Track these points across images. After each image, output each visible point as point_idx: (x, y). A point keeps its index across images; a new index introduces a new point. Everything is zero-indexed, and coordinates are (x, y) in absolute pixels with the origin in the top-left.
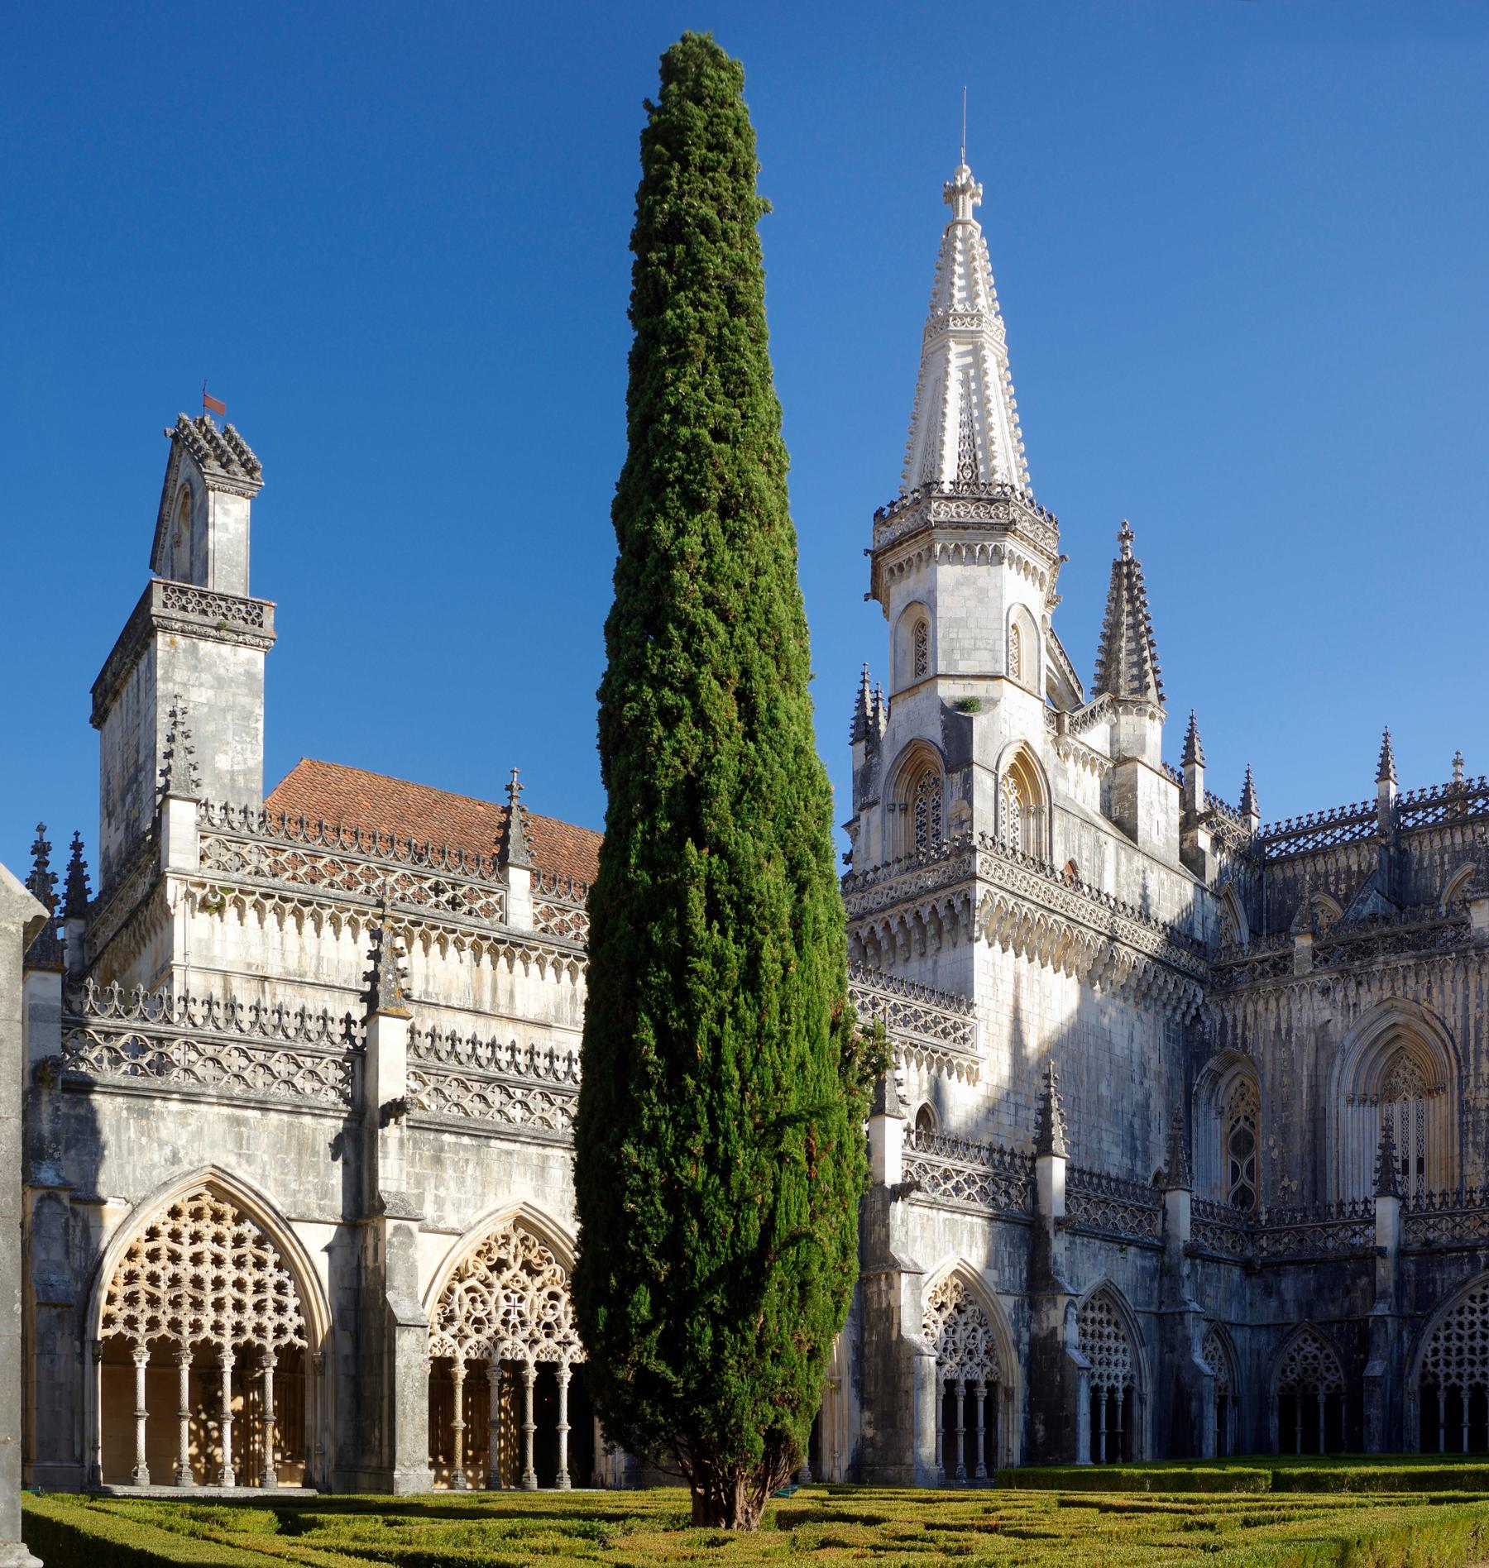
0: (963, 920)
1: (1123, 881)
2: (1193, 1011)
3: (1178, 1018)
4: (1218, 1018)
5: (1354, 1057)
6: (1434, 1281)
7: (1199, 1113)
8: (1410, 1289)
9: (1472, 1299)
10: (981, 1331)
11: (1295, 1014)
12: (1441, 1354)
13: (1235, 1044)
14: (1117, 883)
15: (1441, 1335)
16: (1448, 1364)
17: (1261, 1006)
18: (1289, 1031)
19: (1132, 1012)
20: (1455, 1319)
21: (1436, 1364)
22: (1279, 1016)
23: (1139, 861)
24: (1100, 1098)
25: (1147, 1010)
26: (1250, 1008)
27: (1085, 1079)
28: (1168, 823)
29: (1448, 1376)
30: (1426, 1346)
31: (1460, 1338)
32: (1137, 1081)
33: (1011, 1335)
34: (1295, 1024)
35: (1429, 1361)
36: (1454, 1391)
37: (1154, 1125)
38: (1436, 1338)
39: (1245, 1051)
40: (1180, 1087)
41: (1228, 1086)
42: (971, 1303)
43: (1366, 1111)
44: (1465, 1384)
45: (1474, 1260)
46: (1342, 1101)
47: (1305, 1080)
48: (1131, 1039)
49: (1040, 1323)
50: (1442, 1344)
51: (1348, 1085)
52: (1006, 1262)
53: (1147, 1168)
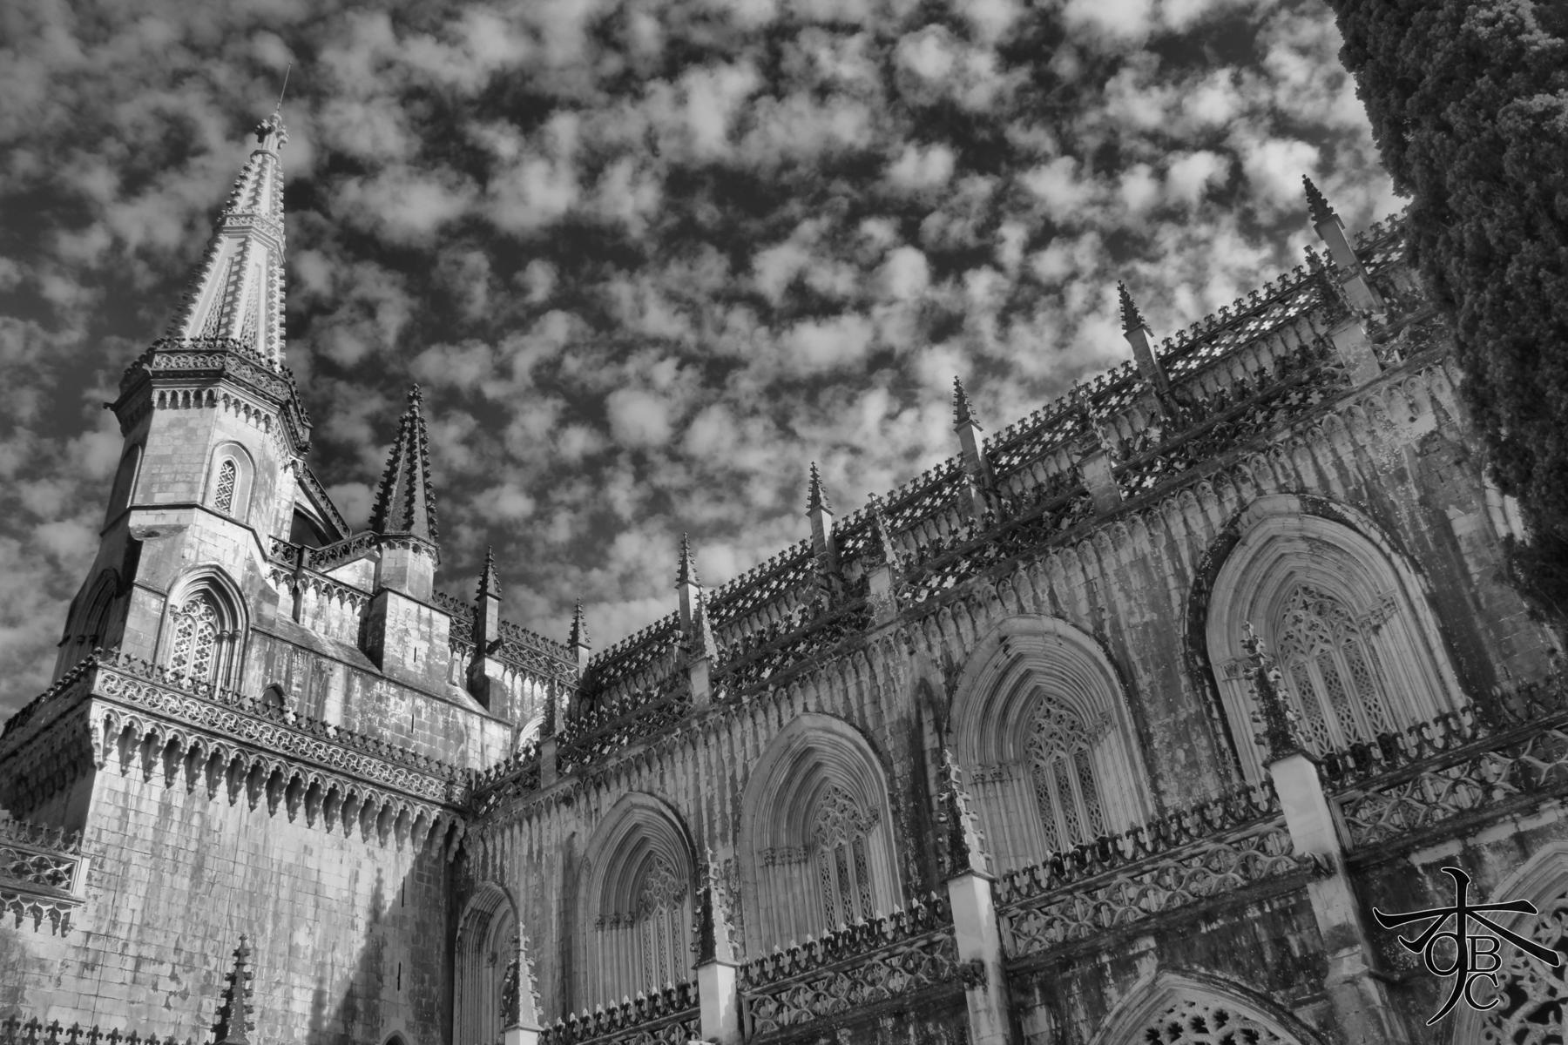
1: (354, 708)
2: (455, 846)
3: (435, 854)
4: (481, 849)
5: (601, 871)
7: (465, 962)
11: (545, 833)
13: (494, 877)
14: (346, 710)
22: (531, 839)
24: (293, 950)
27: (269, 927)
34: (545, 844)
37: (389, 981)
39: (502, 885)
40: (438, 935)
41: (499, 927)
43: (623, 934)
46: (590, 928)
47: (554, 906)
51: (596, 906)
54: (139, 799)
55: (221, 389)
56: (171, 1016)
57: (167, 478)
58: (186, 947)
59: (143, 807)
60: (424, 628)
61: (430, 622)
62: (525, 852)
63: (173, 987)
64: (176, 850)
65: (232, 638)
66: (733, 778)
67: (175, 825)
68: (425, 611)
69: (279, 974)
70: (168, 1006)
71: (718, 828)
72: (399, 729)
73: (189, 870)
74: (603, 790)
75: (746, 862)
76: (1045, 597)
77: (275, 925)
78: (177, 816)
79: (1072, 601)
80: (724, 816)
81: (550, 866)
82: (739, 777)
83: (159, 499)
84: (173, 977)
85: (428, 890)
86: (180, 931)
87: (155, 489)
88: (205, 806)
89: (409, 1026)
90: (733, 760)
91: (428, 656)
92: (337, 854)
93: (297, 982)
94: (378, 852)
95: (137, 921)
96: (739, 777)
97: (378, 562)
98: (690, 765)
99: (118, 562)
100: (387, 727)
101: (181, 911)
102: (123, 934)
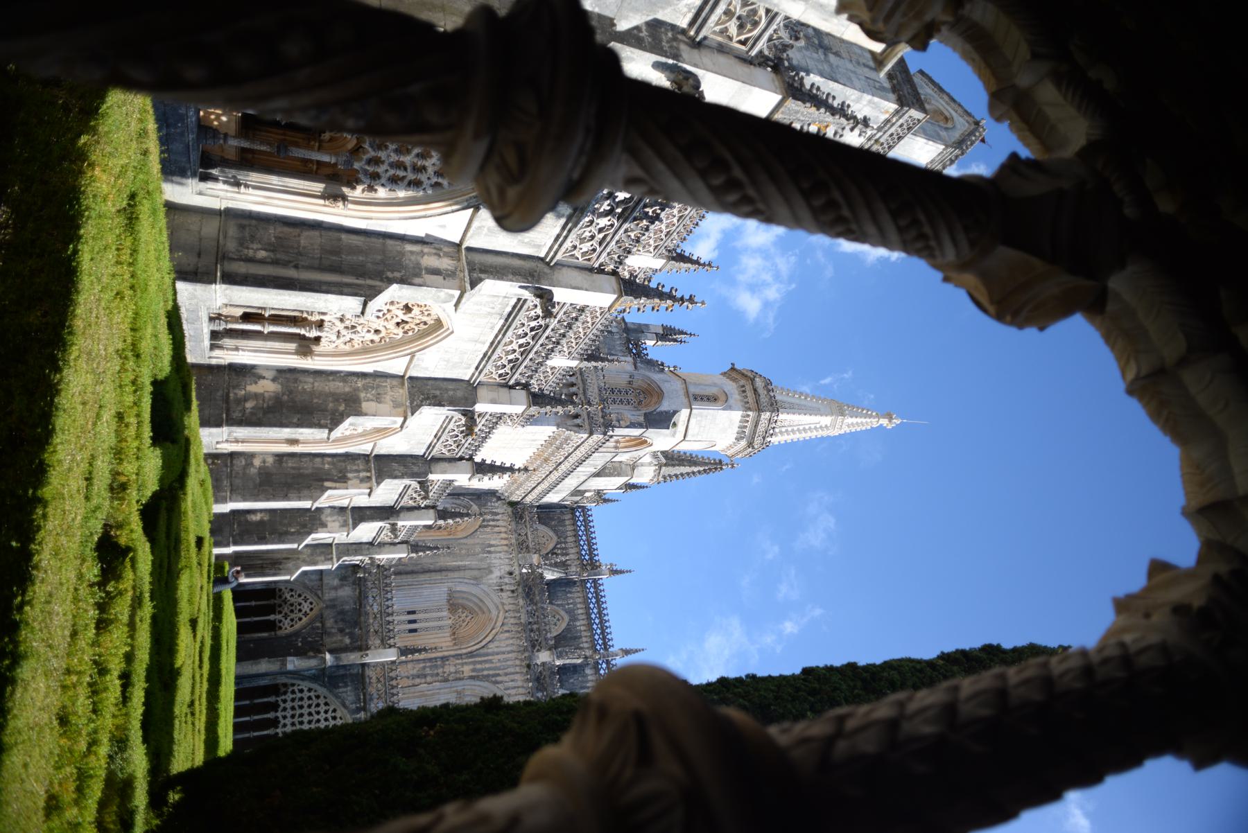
0: (570, 422)
4: (498, 510)
5: (474, 590)
6: (346, 686)
8: (342, 672)
9: (334, 711)
12: (299, 695)
15: (312, 694)
16: (293, 700)
17: (503, 535)
18: (489, 552)
20: (322, 701)
21: (293, 692)
26: (503, 530)
29: (285, 701)
30: (305, 685)
31: (310, 706)
35: (296, 688)
36: (275, 707)
38: (310, 690)
44: (279, 714)
45: (358, 710)
49: (331, 515)
50: (306, 695)
55: (743, 443)
62: (493, 542)
65: (616, 447)
66: (498, 675)
71: (479, 666)
74: (509, 594)
75: (461, 683)
80: (483, 670)
81: (482, 560)
82: (499, 679)
90: (506, 674)
96: (499, 679)
97: (650, 464)
98: (509, 649)
99: (665, 406)
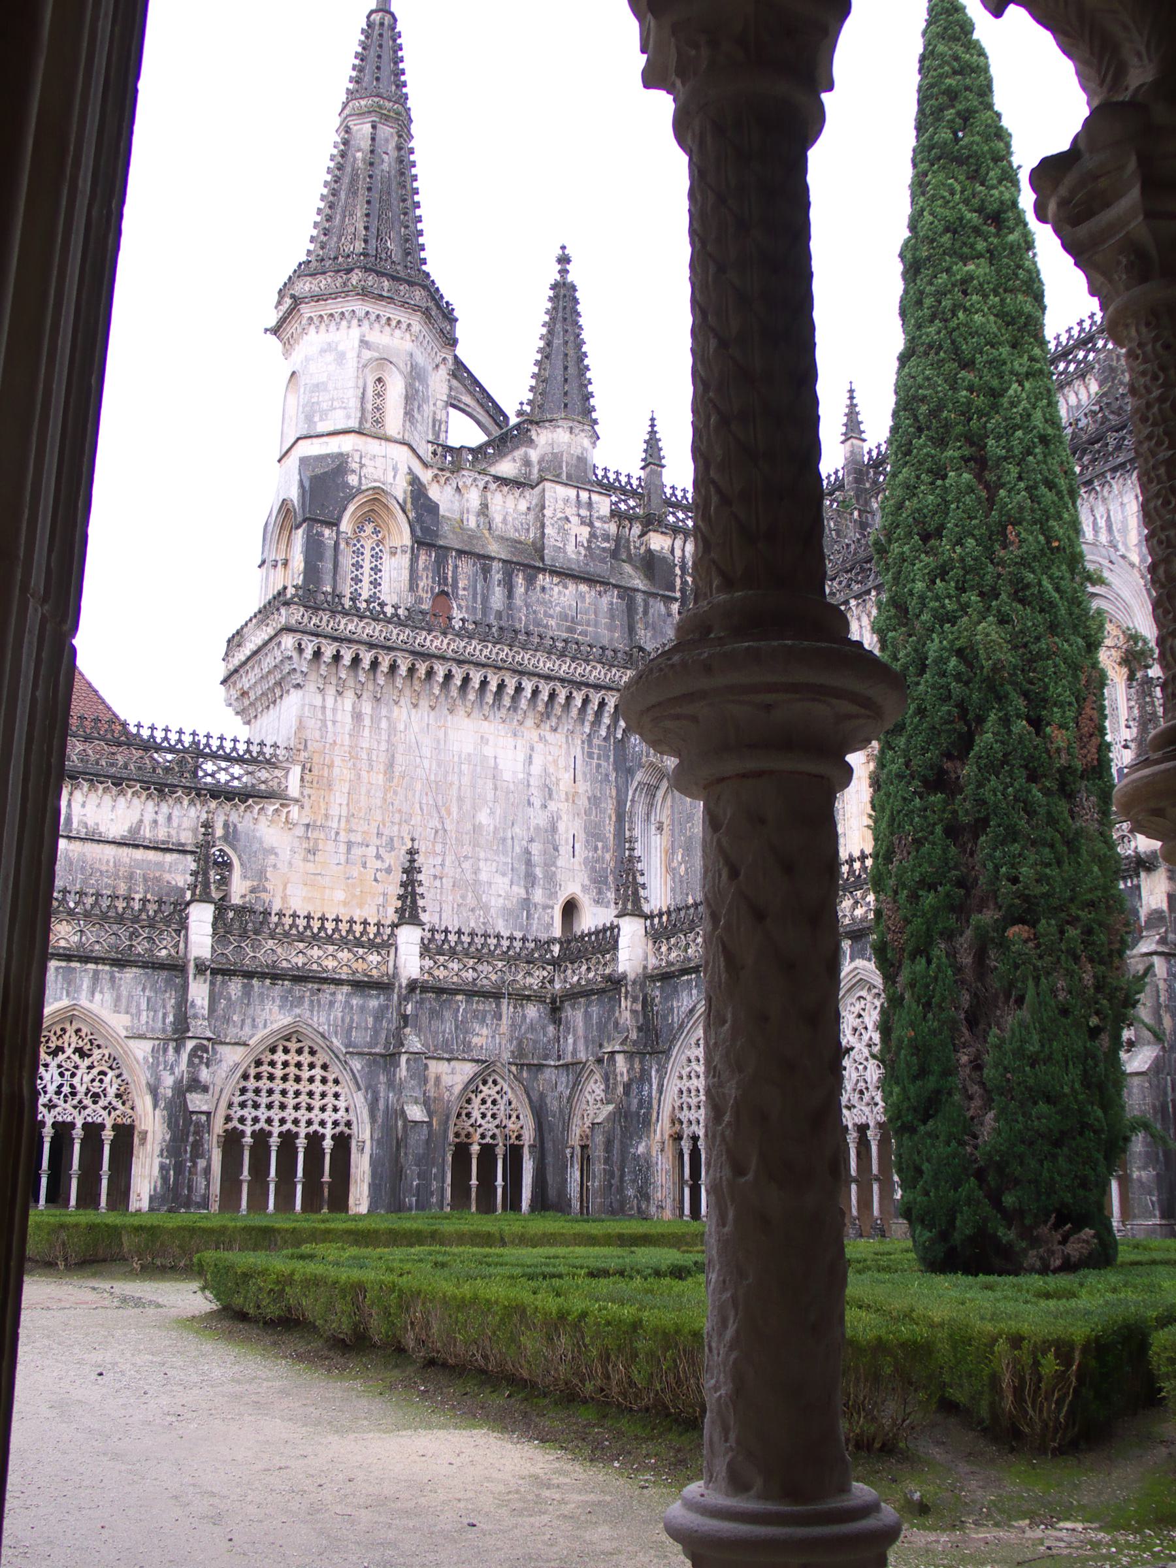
3: (603, 732)
6: (672, 1009)
10: (111, 1074)
15: (684, 1073)
19: (530, 732)
23: (543, 580)
24: (477, 829)
25: (555, 730)
27: (454, 810)
28: (593, 535)
32: (537, 802)
33: (140, 1078)
37: (565, 850)
38: (681, 1078)
40: (610, 806)
42: (99, 1047)
48: (530, 760)
52: (144, 1006)
53: (553, 895)
54: (334, 710)
56: (380, 888)
57: (324, 406)
58: (386, 832)
59: (339, 717)
60: (584, 512)
61: (590, 505)
63: (379, 864)
64: (370, 751)
67: (367, 730)
68: (584, 495)
69: (467, 850)
70: (376, 880)
72: (564, 617)
73: (382, 768)
76: (1102, 523)
77: (460, 808)
78: (367, 721)
79: (1124, 531)
83: (322, 427)
84: (378, 857)
85: (599, 766)
86: (379, 818)
87: (316, 419)
88: (391, 711)
89: (585, 888)
91: (589, 541)
92: (510, 741)
93: (482, 855)
94: (550, 736)
95: (344, 813)
100: (552, 617)
101: (379, 802)
102: (335, 825)
